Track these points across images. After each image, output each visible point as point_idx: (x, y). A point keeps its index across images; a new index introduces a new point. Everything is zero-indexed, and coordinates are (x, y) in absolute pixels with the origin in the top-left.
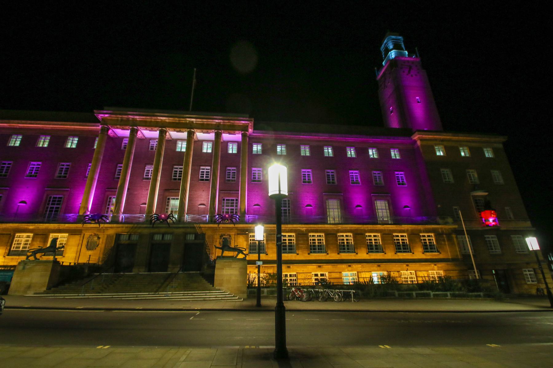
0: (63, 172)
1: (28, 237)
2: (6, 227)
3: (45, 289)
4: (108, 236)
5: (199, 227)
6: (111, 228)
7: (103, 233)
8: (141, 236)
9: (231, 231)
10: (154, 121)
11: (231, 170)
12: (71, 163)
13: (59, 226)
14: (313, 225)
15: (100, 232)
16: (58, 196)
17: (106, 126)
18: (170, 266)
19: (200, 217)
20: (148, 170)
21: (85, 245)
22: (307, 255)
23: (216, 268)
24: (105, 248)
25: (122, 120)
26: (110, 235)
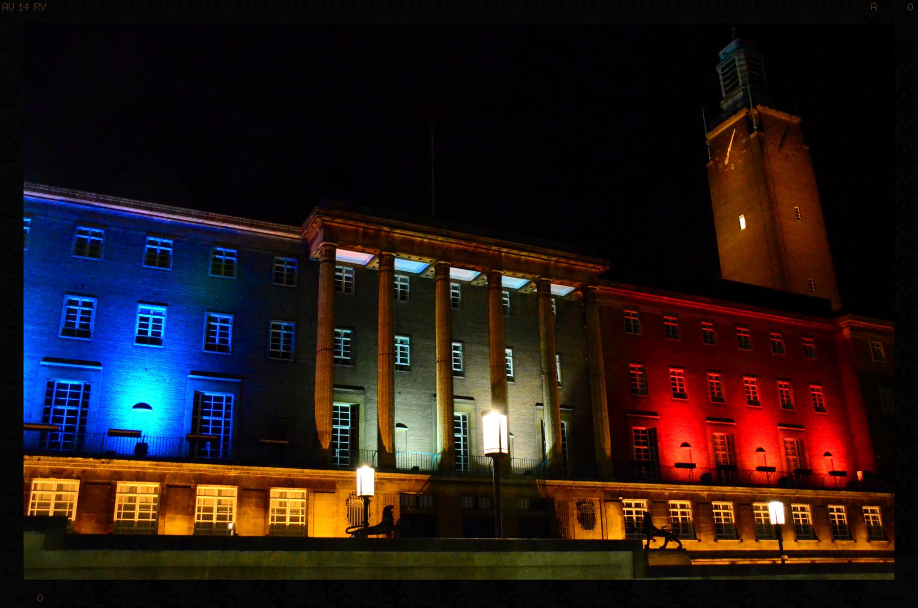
6: (390, 480)
9: (594, 494)
10: (428, 242)
14: (693, 486)
22: (713, 542)
25: (365, 234)
26: (391, 495)
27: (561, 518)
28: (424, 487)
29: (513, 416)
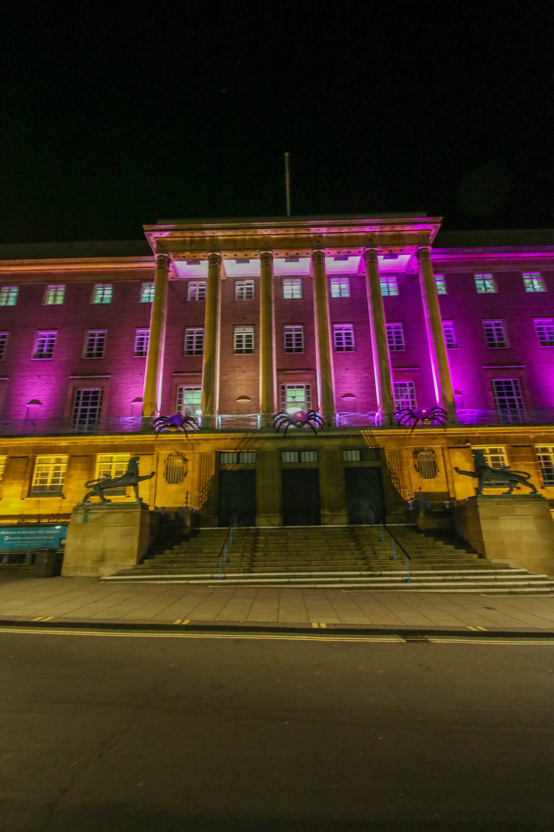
0: (95, 347)
1: (58, 461)
2: (19, 444)
3: (132, 562)
4: (202, 456)
5: (369, 435)
6: (206, 440)
7: (192, 451)
8: (260, 454)
9: (435, 442)
11: (393, 327)
12: (106, 330)
13: (113, 439)
15: (186, 449)
16: (92, 390)
17: (166, 255)
18: (325, 512)
19: (366, 415)
20: (238, 337)
21: (163, 473)
23: (481, 517)
24: (200, 480)
27: (394, 468)
28: (241, 443)
29: (355, 380)
